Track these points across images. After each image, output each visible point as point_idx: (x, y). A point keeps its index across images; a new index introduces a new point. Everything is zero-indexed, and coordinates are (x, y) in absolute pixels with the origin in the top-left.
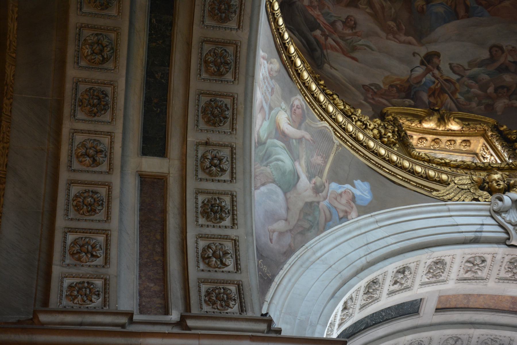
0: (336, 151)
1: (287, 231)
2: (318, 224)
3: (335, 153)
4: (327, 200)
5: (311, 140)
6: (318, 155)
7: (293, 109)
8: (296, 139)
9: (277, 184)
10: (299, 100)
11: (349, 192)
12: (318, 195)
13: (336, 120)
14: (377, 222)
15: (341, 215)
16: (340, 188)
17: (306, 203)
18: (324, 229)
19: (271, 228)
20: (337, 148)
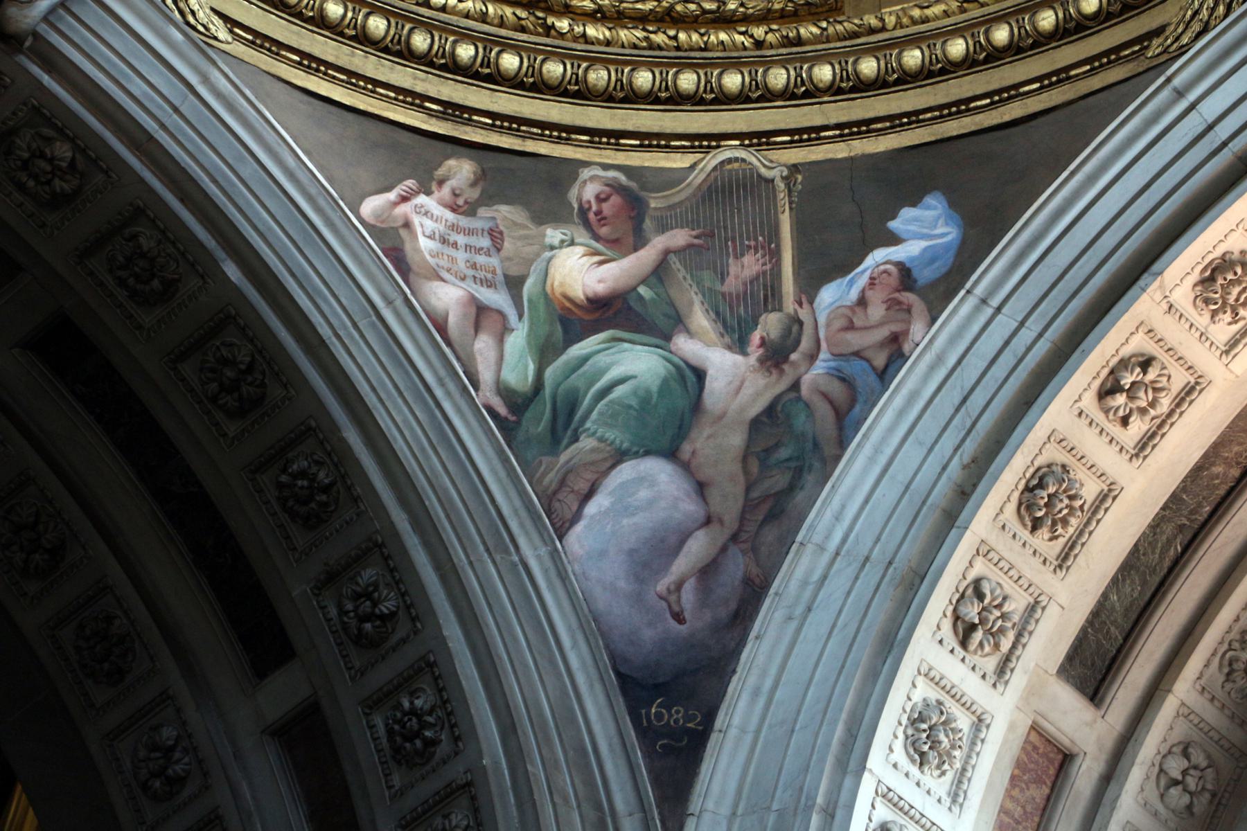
0: (790, 196)
1: (724, 549)
2: (816, 445)
3: (790, 203)
4: (824, 355)
5: (696, 237)
6: (743, 255)
7: (591, 216)
8: (644, 281)
9: (636, 455)
10: (593, 178)
11: (885, 272)
12: (786, 367)
13: (769, 96)
14: (984, 301)
15: (880, 360)
16: (851, 283)
17: (755, 425)
18: (842, 444)
19: (662, 586)
20: (788, 186)
